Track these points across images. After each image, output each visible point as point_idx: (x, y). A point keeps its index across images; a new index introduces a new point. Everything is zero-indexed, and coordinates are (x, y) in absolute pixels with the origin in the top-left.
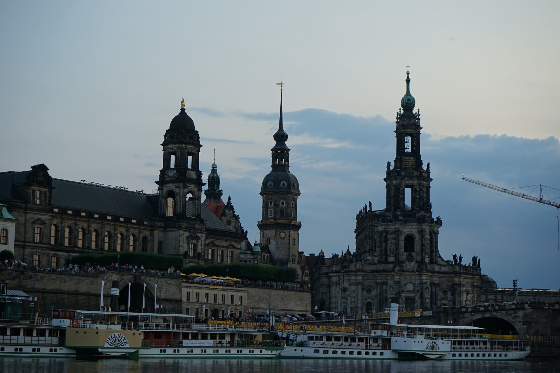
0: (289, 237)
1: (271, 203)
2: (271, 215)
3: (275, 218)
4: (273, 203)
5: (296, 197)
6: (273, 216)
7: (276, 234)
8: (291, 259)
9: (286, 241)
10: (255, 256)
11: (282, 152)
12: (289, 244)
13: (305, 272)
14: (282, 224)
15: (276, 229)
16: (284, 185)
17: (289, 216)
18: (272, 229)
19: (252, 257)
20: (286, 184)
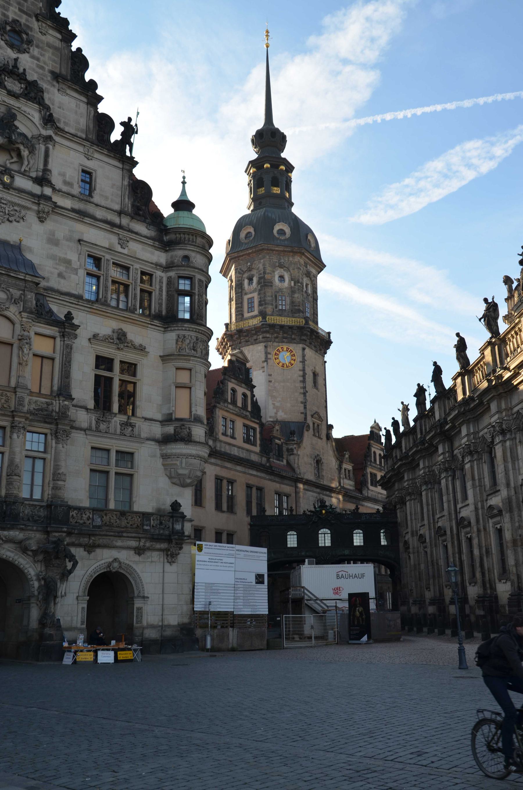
0: (303, 361)
1: (250, 279)
2: (251, 308)
3: (263, 314)
4: (255, 280)
5: (314, 271)
6: (256, 312)
7: (267, 353)
8: (310, 421)
9: (296, 373)
10: (179, 253)
11: (275, 166)
12: (304, 381)
13: (345, 466)
14: (282, 327)
15: (266, 340)
16: (281, 232)
17: (299, 311)
18: (256, 342)
19: (161, 257)
20: (287, 230)
